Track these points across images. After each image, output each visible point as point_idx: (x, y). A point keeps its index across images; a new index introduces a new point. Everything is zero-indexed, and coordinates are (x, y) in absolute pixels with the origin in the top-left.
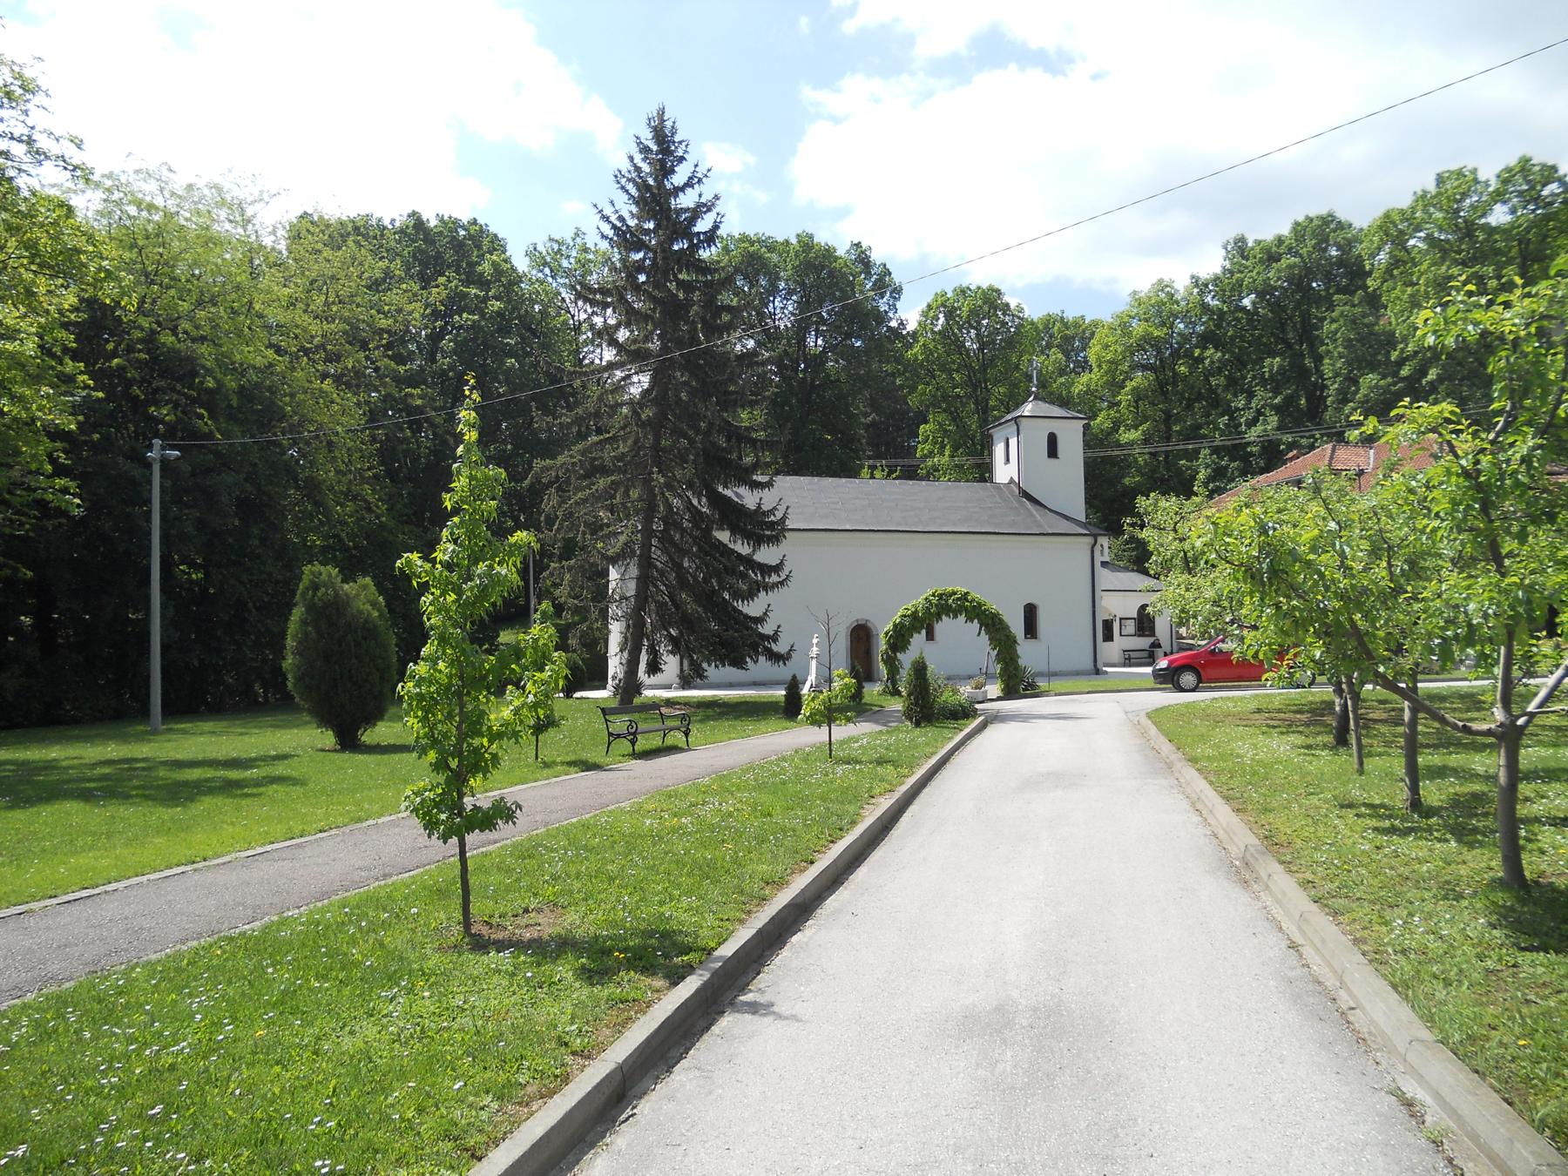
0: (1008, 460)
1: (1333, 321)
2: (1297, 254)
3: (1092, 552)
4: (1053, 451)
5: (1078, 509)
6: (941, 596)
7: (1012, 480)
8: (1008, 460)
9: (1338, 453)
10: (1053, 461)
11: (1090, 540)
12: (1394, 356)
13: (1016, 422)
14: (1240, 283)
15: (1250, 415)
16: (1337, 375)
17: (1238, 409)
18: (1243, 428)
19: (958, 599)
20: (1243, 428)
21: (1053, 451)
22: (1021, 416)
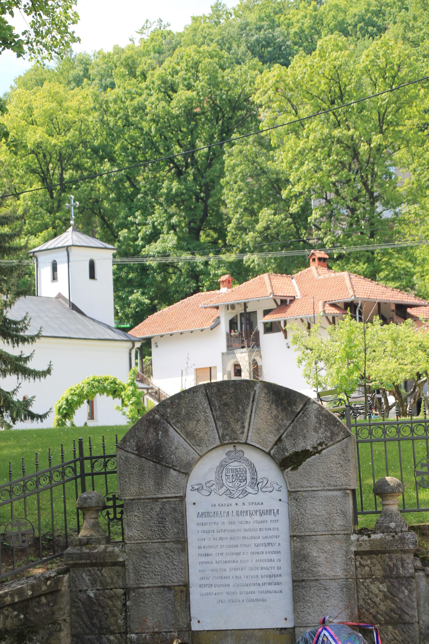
0: (54, 278)
1: (231, 155)
2: (189, 87)
3: (130, 354)
4: (92, 276)
5: (112, 322)
6: (98, 381)
7: (60, 296)
8: (54, 278)
9: (274, 281)
10: (92, 281)
11: (130, 345)
12: (284, 194)
13: (67, 250)
14: (141, 108)
15: (147, 230)
16: (238, 205)
17: (133, 224)
18: (140, 242)
19: (111, 383)
20: (140, 242)
21: (92, 276)
22: (73, 246)
